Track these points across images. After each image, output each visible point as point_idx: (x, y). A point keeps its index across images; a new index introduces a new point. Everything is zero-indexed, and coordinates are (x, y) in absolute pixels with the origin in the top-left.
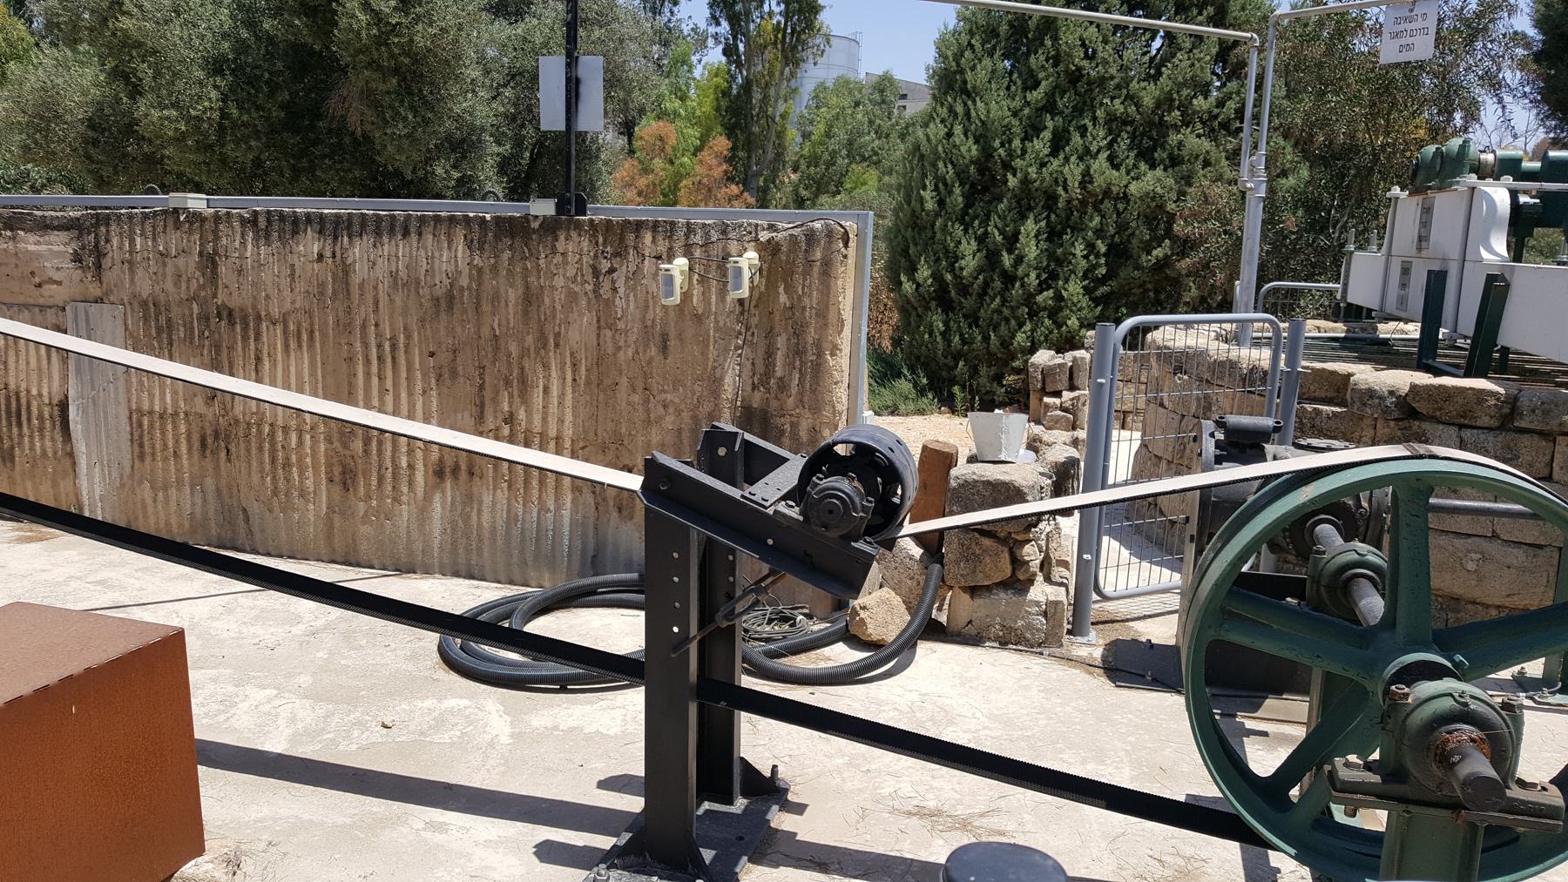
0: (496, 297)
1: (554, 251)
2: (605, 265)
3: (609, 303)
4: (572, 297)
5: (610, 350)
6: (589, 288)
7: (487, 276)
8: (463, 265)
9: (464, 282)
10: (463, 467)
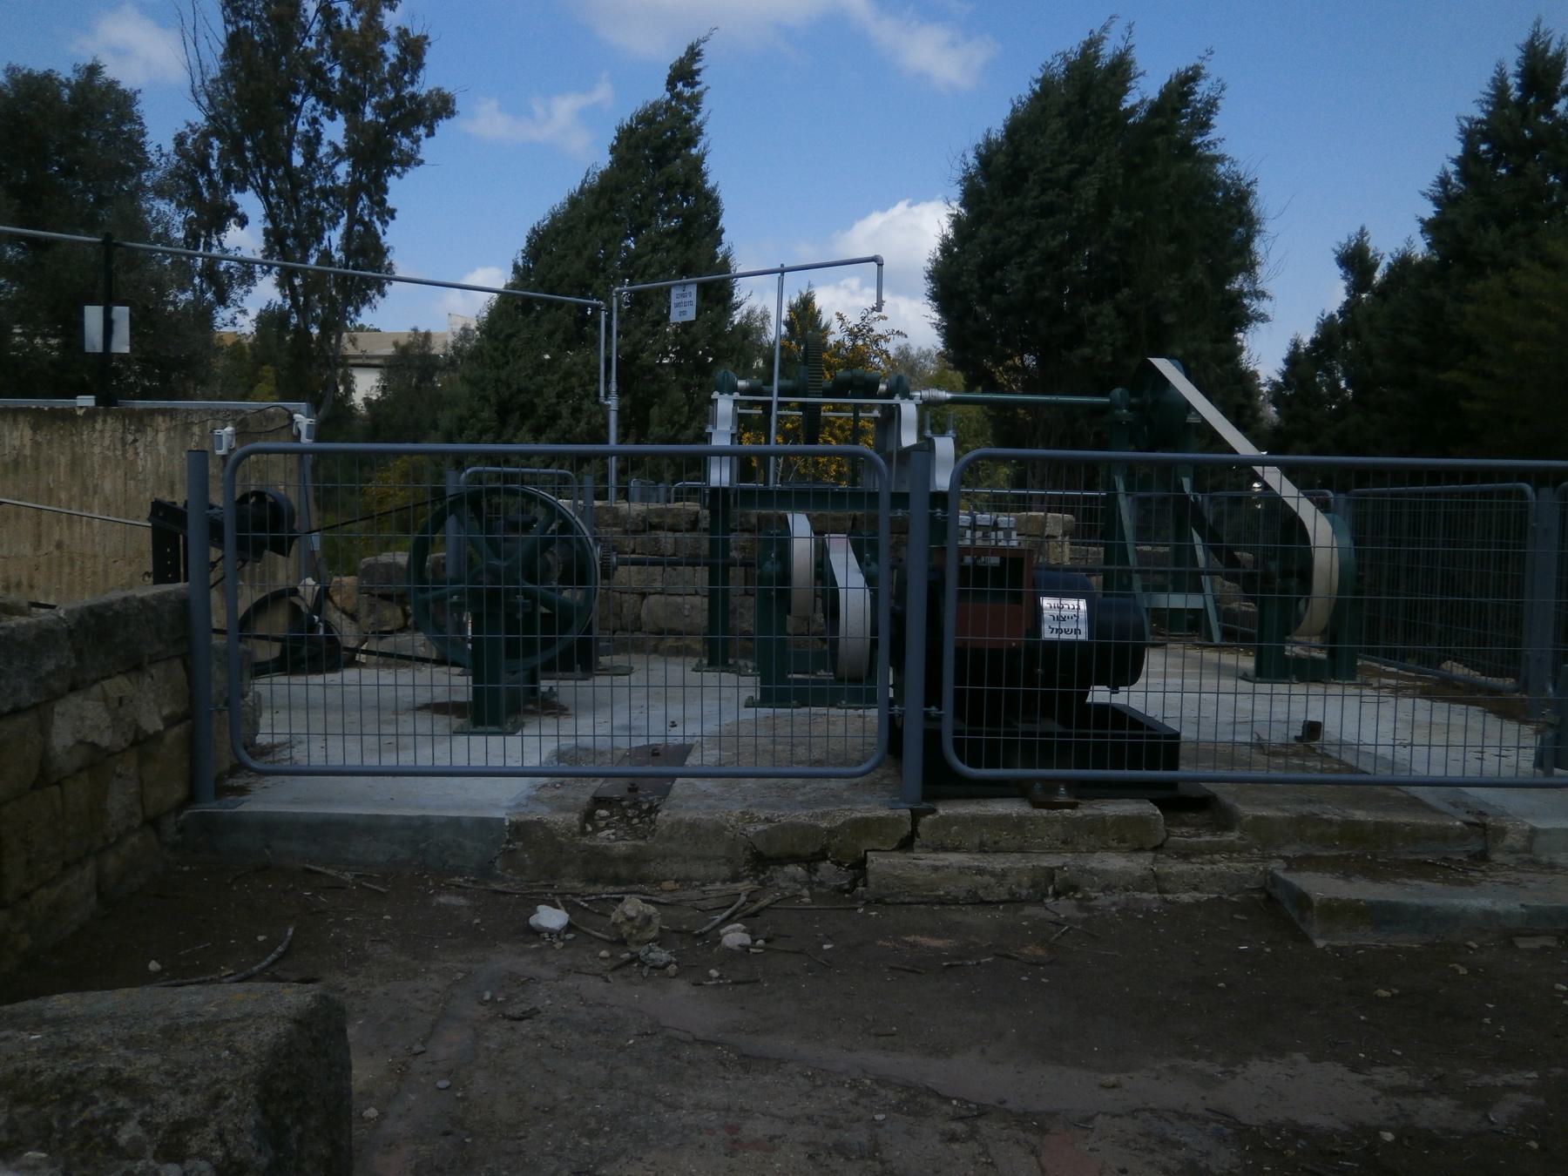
0: (51, 462)
1: (94, 430)
2: (130, 438)
3: (133, 463)
4: (106, 459)
6: (118, 453)
7: (45, 446)
8: (27, 441)
9: (27, 452)
10: (25, 582)
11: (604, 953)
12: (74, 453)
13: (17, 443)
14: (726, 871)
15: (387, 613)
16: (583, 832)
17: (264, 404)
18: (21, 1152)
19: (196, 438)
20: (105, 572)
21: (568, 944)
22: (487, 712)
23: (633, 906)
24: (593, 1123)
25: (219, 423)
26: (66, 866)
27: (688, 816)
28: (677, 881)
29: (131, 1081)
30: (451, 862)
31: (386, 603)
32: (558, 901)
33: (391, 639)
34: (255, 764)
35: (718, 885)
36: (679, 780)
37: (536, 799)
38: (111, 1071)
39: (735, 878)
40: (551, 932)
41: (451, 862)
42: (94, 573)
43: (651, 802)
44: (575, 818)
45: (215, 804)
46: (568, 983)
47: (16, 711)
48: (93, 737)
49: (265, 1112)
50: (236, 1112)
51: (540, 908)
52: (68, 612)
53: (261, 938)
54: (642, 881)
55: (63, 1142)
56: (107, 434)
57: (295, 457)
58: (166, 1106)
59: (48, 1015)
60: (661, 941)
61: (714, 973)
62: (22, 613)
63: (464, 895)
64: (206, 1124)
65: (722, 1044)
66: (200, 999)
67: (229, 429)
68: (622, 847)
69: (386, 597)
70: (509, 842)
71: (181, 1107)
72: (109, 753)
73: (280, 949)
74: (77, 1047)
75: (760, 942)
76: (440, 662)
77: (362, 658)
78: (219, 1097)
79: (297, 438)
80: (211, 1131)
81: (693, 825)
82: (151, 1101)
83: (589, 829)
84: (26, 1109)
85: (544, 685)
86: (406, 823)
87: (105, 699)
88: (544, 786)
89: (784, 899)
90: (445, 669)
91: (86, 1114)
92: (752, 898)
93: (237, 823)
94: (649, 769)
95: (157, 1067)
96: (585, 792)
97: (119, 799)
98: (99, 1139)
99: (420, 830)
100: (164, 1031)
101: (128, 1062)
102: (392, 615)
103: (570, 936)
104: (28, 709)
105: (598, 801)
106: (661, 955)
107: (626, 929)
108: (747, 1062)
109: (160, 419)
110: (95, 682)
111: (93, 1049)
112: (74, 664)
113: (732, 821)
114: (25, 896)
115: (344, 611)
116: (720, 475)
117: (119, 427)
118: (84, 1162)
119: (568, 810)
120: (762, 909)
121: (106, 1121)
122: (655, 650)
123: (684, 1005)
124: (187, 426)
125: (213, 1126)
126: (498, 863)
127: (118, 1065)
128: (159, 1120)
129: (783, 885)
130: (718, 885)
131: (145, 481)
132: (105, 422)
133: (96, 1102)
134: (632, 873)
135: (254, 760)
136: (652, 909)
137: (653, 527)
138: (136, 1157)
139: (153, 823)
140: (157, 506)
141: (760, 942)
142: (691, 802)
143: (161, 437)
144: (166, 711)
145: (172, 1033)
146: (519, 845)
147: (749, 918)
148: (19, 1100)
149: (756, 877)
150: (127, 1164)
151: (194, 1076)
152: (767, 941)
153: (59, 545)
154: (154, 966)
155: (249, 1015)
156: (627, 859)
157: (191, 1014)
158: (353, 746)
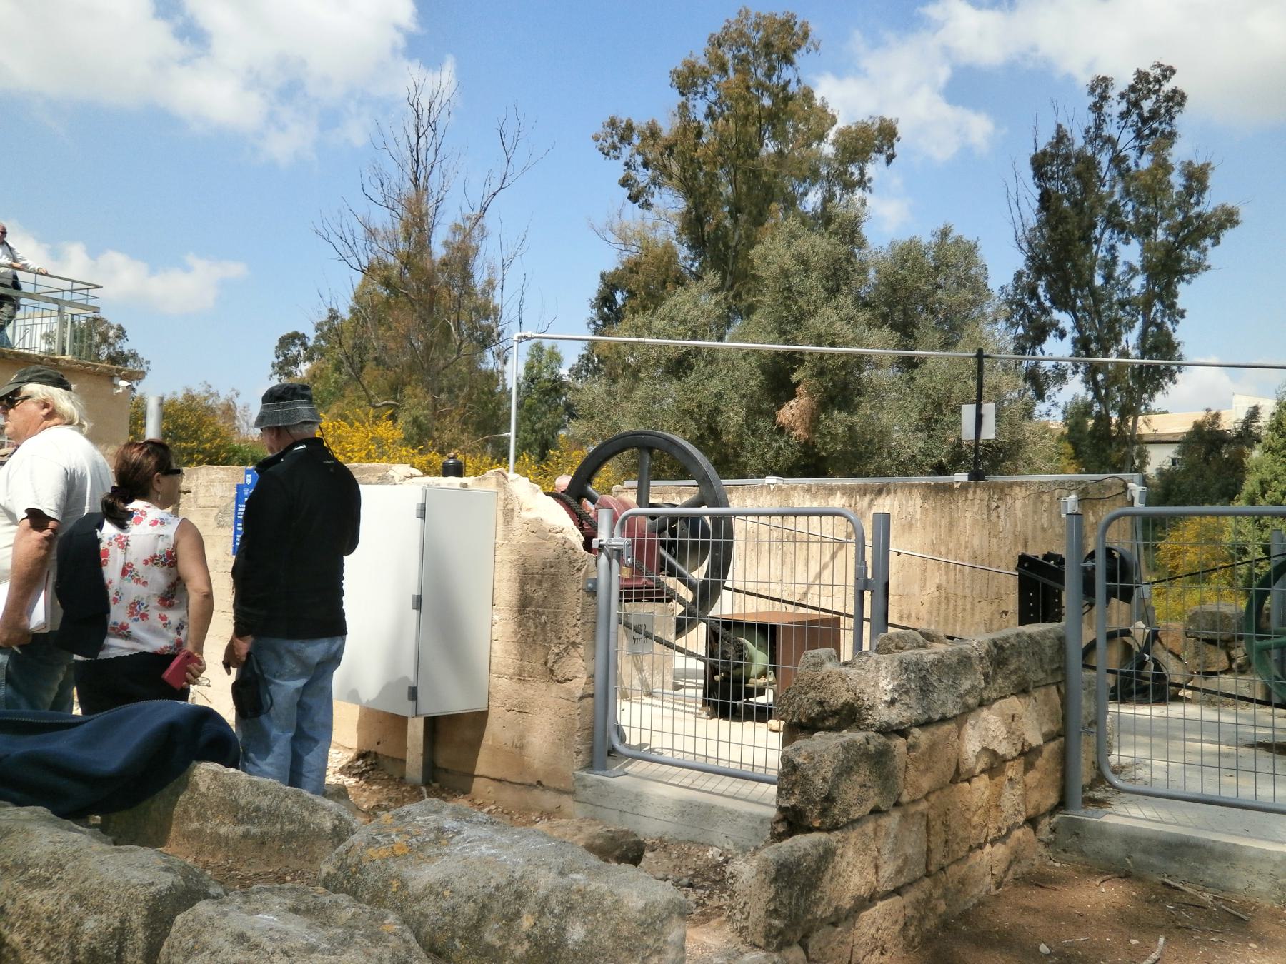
2: (994, 505)
3: (995, 524)
5: (995, 548)
9: (918, 516)
12: (951, 518)
13: (911, 510)
15: (1213, 656)
17: (1102, 476)
19: (1046, 504)
25: (1065, 492)
31: (1212, 647)
33: (1215, 679)
34: (1117, 782)
45: (1082, 812)
47: (944, 720)
52: (979, 643)
53: (1134, 942)
56: (977, 502)
57: (1129, 518)
62: (941, 642)
72: (1004, 760)
76: (1266, 703)
77: (1188, 693)
79: (1131, 503)
90: (1269, 710)
93: (1102, 832)
109: (1017, 489)
110: (995, 700)
112: (983, 685)
114: (942, 869)
115: (1171, 652)
117: (986, 496)
124: (1039, 495)
131: (1005, 538)
132: (975, 492)
140: (1023, 559)
143: (1018, 504)
144: (1045, 729)
153: (939, 588)
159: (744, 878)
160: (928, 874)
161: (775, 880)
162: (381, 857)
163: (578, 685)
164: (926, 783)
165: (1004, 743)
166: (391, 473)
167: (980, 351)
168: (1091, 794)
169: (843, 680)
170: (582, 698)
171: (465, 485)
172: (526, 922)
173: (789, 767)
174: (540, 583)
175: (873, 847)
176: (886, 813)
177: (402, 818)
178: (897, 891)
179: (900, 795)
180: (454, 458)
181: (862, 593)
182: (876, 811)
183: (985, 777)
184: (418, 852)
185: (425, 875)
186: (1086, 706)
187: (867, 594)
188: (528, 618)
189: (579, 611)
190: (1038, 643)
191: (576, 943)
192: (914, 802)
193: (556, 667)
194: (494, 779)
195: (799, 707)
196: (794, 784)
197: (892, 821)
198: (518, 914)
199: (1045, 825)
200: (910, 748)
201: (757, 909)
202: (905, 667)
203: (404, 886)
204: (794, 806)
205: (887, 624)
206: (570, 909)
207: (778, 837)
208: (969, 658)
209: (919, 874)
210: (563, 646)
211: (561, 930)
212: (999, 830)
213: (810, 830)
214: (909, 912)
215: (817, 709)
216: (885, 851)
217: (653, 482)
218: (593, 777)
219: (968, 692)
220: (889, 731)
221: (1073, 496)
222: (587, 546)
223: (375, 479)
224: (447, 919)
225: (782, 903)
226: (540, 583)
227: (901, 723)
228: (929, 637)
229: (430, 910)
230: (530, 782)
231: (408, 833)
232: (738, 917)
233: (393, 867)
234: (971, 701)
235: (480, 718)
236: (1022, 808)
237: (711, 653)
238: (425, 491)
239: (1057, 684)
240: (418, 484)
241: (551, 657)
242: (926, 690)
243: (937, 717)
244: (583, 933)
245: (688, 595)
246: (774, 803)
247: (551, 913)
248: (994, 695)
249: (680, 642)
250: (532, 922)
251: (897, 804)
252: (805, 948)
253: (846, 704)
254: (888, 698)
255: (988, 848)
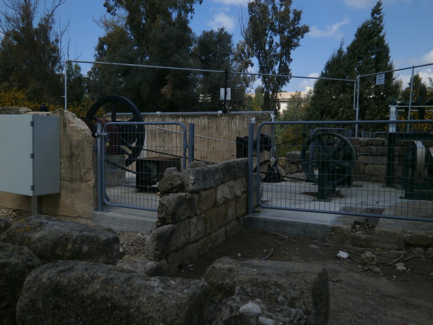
0: (212, 127)
2: (230, 121)
4: (224, 126)
9: (207, 125)
11: (359, 267)
12: (217, 125)
13: (204, 123)
14: (396, 247)
16: (352, 231)
18: (255, 299)
20: (223, 155)
21: (349, 263)
22: (321, 196)
23: (368, 254)
24: (360, 315)
26: (219, 227)
27: (385, 230)
28: (380, 248)
29: (280, 285)
30: (314, 236)
32: (345, 250)
33: (294, 174)
34: (263, 205)
35: (394, 251)
36: (381, 219)
37: (338, 221)
38: (275, 281)
39: (400, 249)
40: (343, 259)
41: (314, 236)
42: (221, 155)
43: (372, 225)
44: (350, 227)
45: (252, 215)
46: (350, 274)
47: (210, 188)
48: (226, 196)
49: (313, 299)
50: (307, 297)
51: (340, 251)
52: (222, 164)
53: (265, 251)
54: (370, 247)
55: (265, 298)
56: (225, 120)
57: (270, 125)
58: (290, 293)
59: (254, 265)
60: (377, 265)
61: (395, 277)
62: (210, 164)
63: (317, 245)
64: (300, 299)
65: (399, 298)
66: (291, 266)
67: (254, 118)
68: (364, 237)
69: (293, 163)
70: (330, 232)
71: (294, 294)
72: (229, 200)
73: (270, 254)
74: (265, 274)
75: (409, 270)
76: (307, 181)
78: (302, 293)
79: (271, 120)
80: (302, 301)
81: (386, 233)
82: (286, 291)
83: (354, 230)
84: (255, 288)
85: (337, 189)
86: (302, 224)
87: (229, 186)
88: (340, 217)
89: (416, 258)
90: (309, 183)
91: (270, 292)
92: (405, 256)
93: (258, 220)
94: (371, 215)
95: (286, 282)
96: (353, 220)
97: (231, 212)
98: (273, 299)
99: (305, 226)
100: (286, 273)
101: (279, 280)
102: (294, 168)
103: (349, 260)
104: (212, 188)
105: (356, 223)
106: (378, 269)
107: (366, 261)
108: (408, 305)
109: (237, 116)
110: (226, 182)
111: (269, 275)
112: (222, 177)
113: (399, 232)
114: (210, 234)
116: (392, 129)
118: (270, 304)
119: (347, 224)
120: (409, 260)
121: (275, 294)
122: (369, 181)
123: (385, 285)
124: (244, 118)
125: (302, 301)
126: (327, 238)
127: (277, 280)
128: (288, 296)
129: (415, 253)
130: (394, 251)
133: (272, 289)
134: (367, 245)
135: (260, 205)
136: (374, 256)
137: (371, 145)
138: (284, 305)
139: (238, 218)
140: (238, 138)
141: (409, 270)
142: (384, 225)
143: (238, 121)
144: (242, 190)
145: (288, 274)
146: (333, 233)
147: (405, 262)
148: (253, 285)
149: (406, 250)
150: (281, 307)
151: (296, 286)
152: (411, 269)
153: (213, 148)
154: (239, 255)
155: (306, 272)
156: (365, 240)
157: (291, 269)
158: (283, 202)
159: (147, 240)
160: (205, 235)
161: (157, 240)
162: (21, 232)
163: (92, 183)
164: (205, 208)
165: (229, 195)
166: (20, 110)
167: (226, 70)
168: (255, 209)
169: (179, 177)
170: (93, 187)
171: (48, 115)
172: (70, 246)
173: (162, 205)
174: (77, 148)
175: (188, 228)
176: (192, 217)
177: (28, 220)
178: (196, 241)
179: (196, 212)
180: (44, 105)
181: (185, 149)
182: (189, 217)
183: (223, 205)
184: (34, 229)
185: (38, 235)
186: (254, 183)
187: (187, 149)
188: (74, 161)
189: (91, 157)
190: (240, 164)
191: (85, 251)
192: (201, 214)
193: (84, 177)
194: (64, 216)
195: (165, 186)
196: (163, 210)
197: (194, 220)
198: (67, 244)
199: (241, 219)
200: (200, 197)
201: (151, 249)
202: (198, 172)
203: (30, 239)
204: (163, 217)
205: (194, 160)
206: (83, 242)
207: (158, 227)
208: (218, 169)
209: (202, 236)
210: (86, 170)
211: (81, 248)
212: (228, 221)
213: (168, 224)
214: (200, 247)
215: (170, 186)
216: (192, 229)
217: (117, 114)
218: (98, 213)
219: (217, 179)
220: (192, 192)
221: (254, 118)
222: (93, 135)
223: (14, 113)
224: (44, 248)
225: (159, 246)
226: (77, 148)
227: (197, 189)
228: (207, 163)
229: (39, 246)
230: (76, 215)
231: (30, 224)
232: (146, 252)
233: (26, 234)
234: (219, 182)
235: (57, 196)
236: (234, 214)
237: (137, 170)
238: (33, 117)
239: (246, 176)
240: (30, 114)
241: (82, 174)
242: (205, 179)
243: (208, 187)
244: (87, 248)
245: (130, 152)
246: (157, 217)
247: (77, 243)
248: (226, 180)
249: (127, 168)
250: (71, 246)
251: (196, 215)
252: (167, 259)
253: (179, 184)
254: (192, 182)
255: (224, 227)
